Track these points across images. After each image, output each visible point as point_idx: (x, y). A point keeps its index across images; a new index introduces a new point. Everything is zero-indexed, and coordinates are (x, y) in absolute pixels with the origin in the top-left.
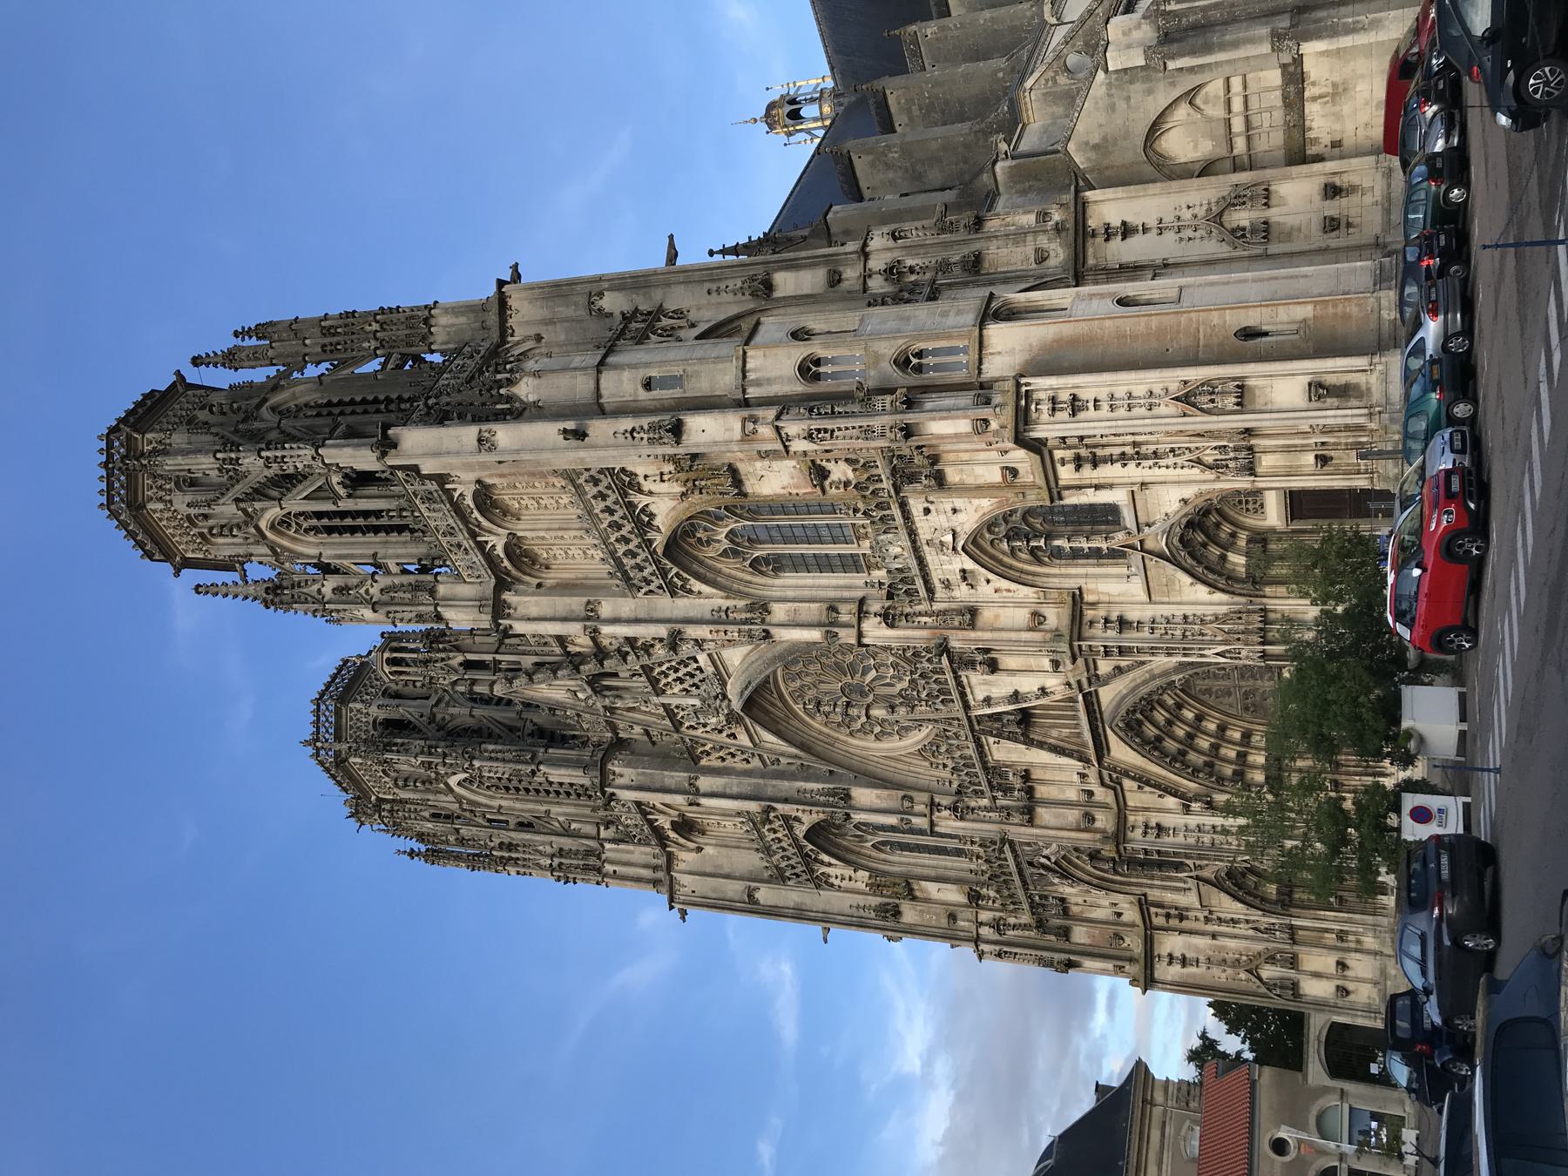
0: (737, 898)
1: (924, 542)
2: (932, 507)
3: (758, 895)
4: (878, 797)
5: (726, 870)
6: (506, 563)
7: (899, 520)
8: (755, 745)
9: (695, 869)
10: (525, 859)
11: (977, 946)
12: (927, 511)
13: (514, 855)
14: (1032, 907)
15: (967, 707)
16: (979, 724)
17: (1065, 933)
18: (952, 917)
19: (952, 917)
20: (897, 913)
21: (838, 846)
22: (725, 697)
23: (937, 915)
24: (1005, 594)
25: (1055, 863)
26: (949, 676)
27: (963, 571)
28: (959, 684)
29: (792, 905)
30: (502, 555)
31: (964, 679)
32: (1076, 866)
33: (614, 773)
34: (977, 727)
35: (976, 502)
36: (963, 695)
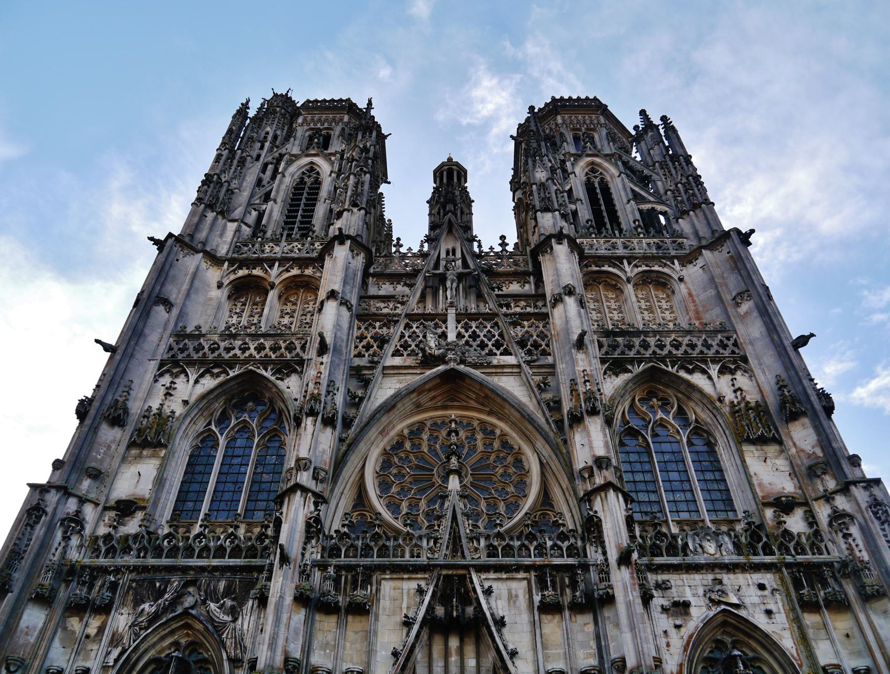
0: (163, 290)
1: (719, 576)
2: (766, 593)
3: (160, 309)
4: (324, 452)
5: (193, 296)
6: (595, 268)
7: (756, 559)
8: (384, 368)
9: (199, 274)
10: (231, 165)
11: (58, 488)
12: (762, 587)
13: (235, 162)
14: (92, 568)
15: (482, 569)
16: (445, 576)
17: (44, 599)
18: (96, 475)
19: (96, 475)
20: (117, 419)
21: (217, 397)
22: (462, 362)
23: (101, 461)
24: (664, 640)
25: (186, 613)
26: (533, 560)
27: (686, 605)
28: (519, 568)
29: (147, 331)
30: (603, 268)
31: (521, 575)
32: (163, 638)
33: (357, 255)
34: (444, 572)
35: (787, 634)
36: (498, 568)
